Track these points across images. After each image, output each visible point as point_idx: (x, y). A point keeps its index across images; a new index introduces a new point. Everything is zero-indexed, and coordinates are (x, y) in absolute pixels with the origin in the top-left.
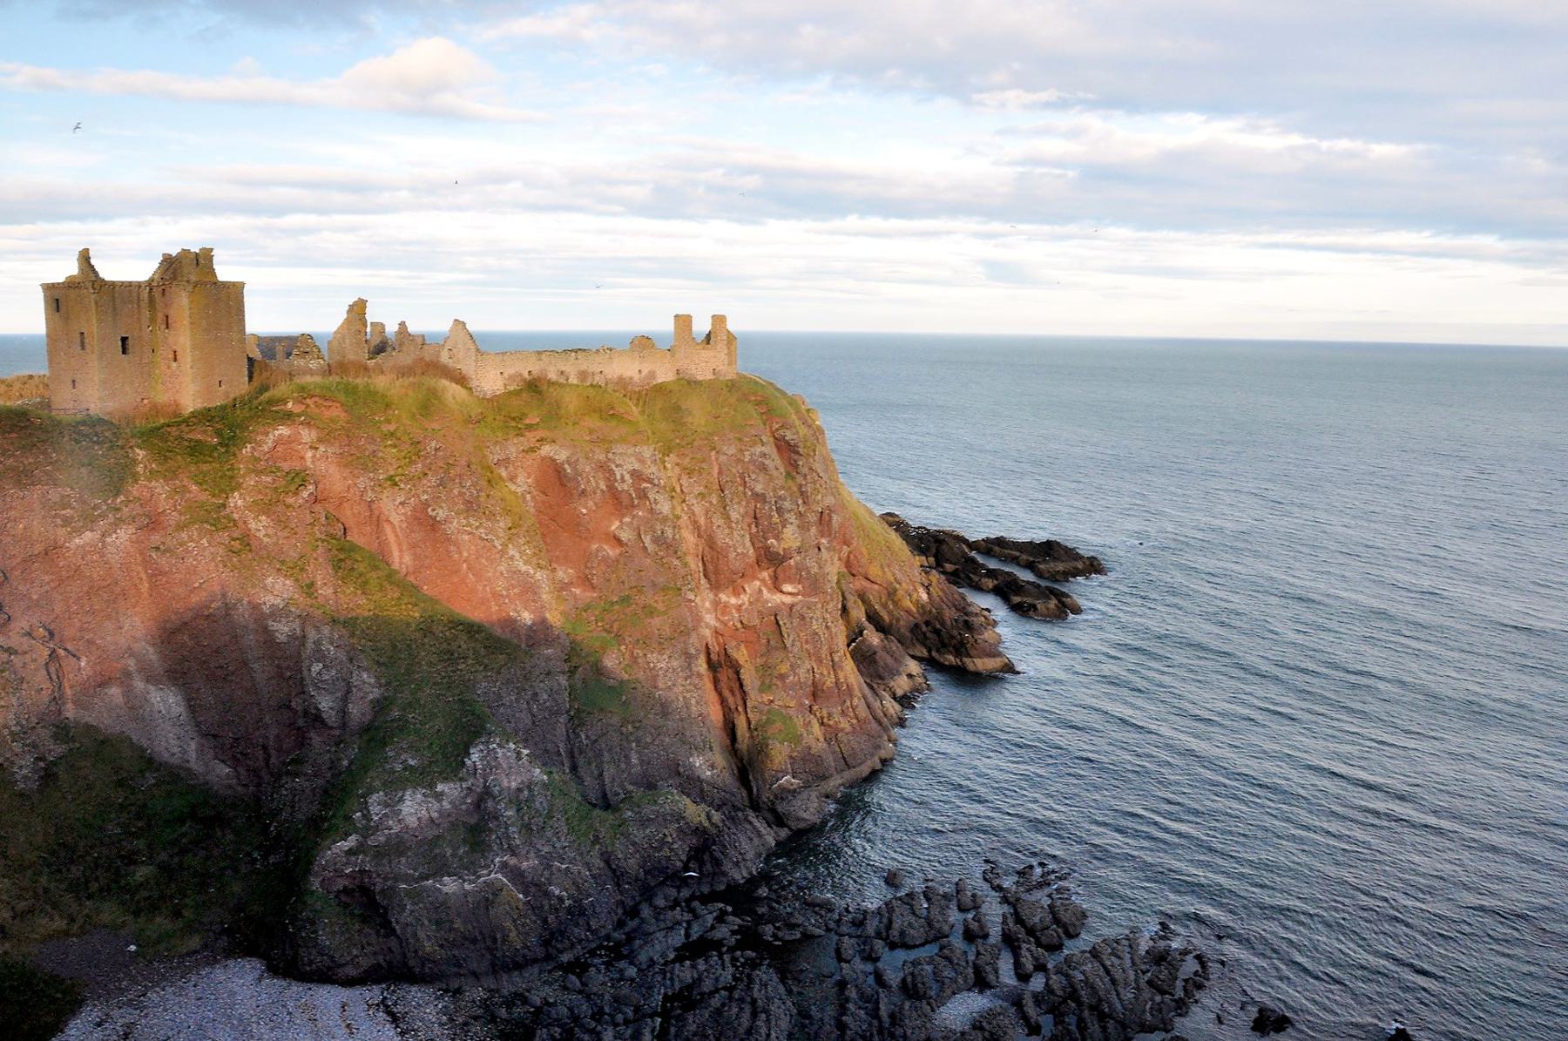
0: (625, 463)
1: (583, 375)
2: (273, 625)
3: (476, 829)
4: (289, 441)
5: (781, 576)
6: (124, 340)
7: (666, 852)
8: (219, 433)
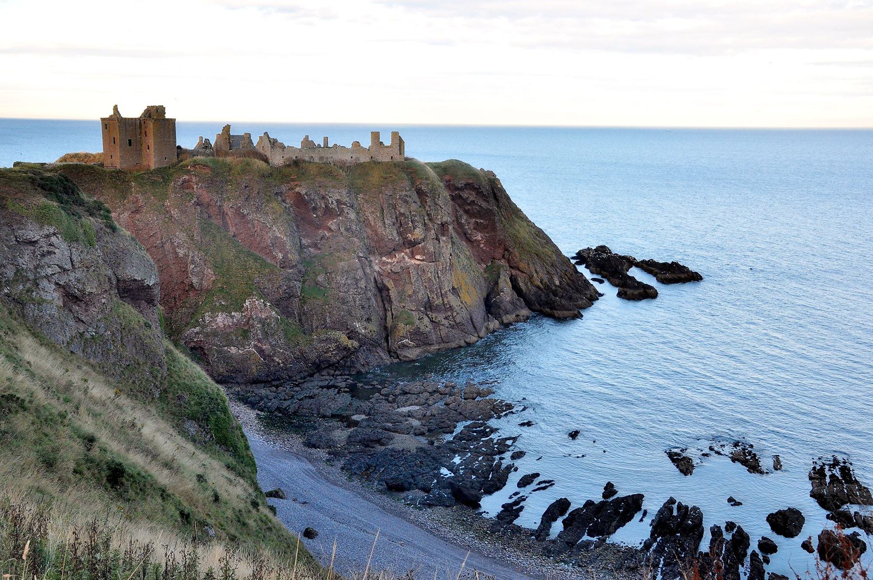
0: (334, 196)
1: (321, 158)
2: (178, 250)
4: (189, 181)
5: (415, 252)
6: (130, 141)
7: (330, 354)
8: (163, 178)
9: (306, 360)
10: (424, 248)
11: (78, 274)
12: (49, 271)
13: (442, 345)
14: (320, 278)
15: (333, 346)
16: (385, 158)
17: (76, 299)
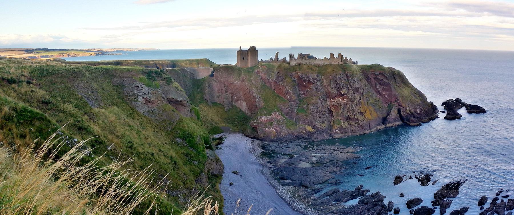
3: (271, 123)
9: (293, 135)
10: (347, 96)
11: (150, 95)
12: (141, 94)
13: (353, 133)
14: (304, 106)
15: (304, 131)
16: (335, 63)
17: (149, 102)
